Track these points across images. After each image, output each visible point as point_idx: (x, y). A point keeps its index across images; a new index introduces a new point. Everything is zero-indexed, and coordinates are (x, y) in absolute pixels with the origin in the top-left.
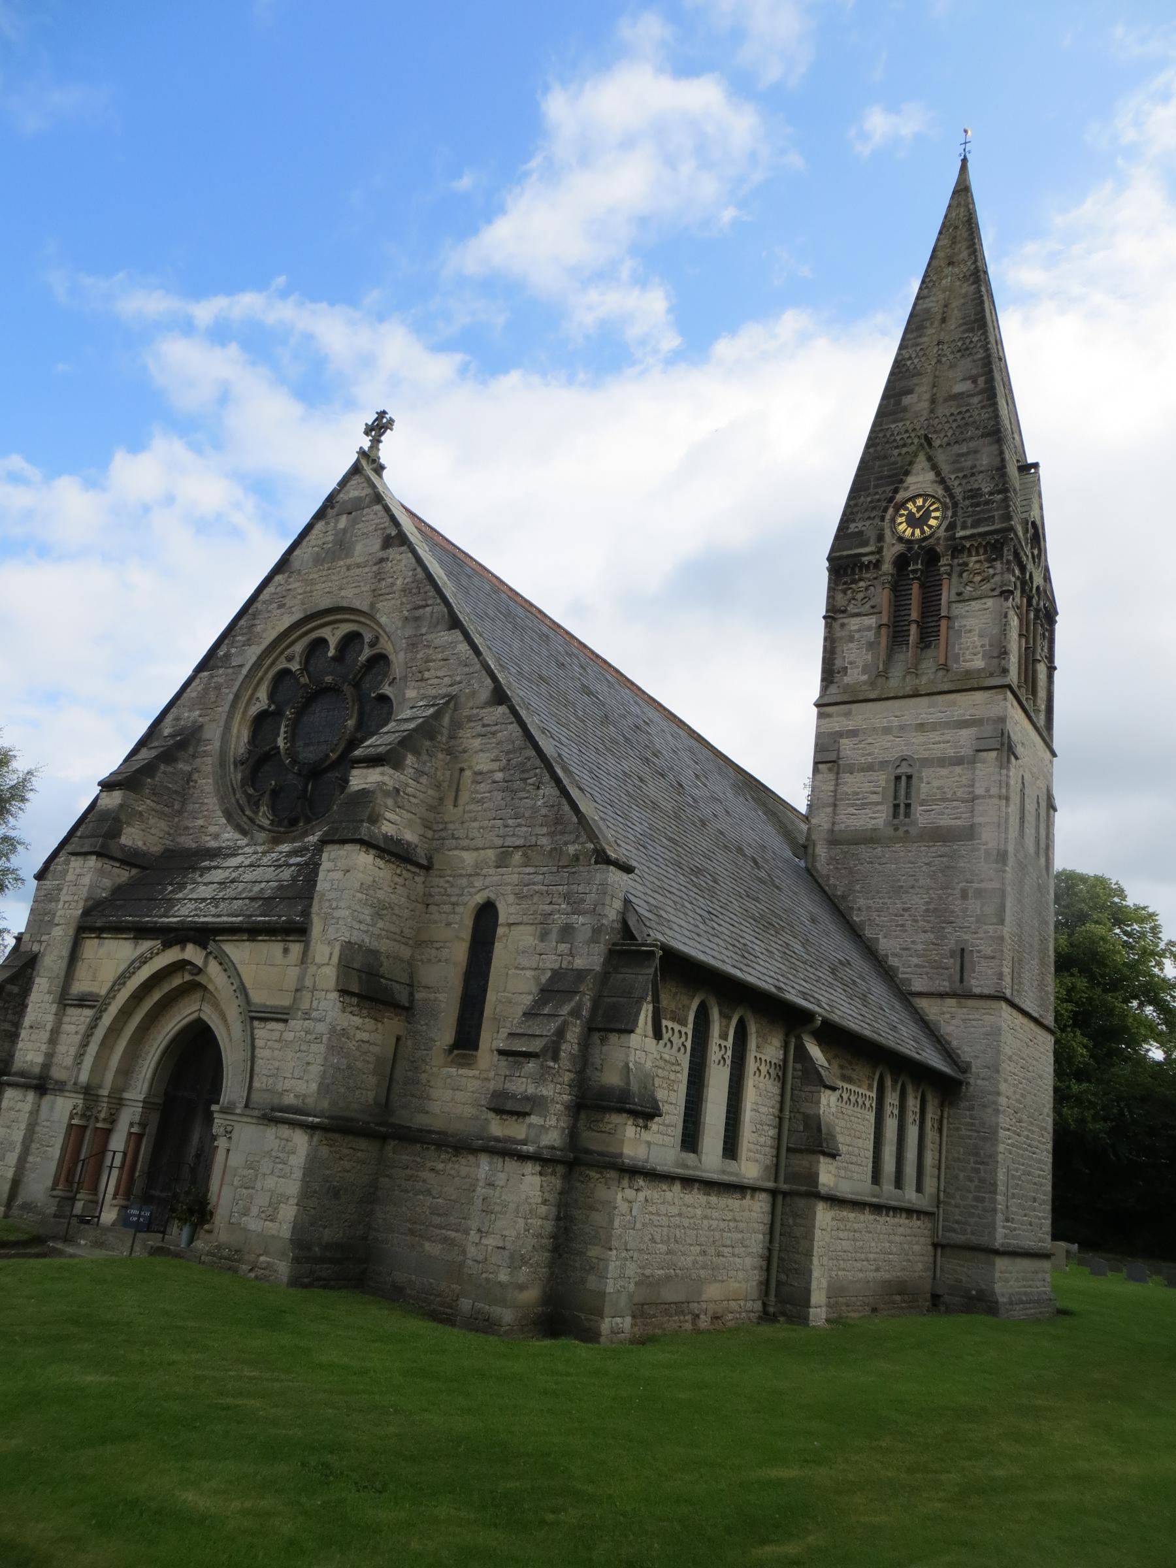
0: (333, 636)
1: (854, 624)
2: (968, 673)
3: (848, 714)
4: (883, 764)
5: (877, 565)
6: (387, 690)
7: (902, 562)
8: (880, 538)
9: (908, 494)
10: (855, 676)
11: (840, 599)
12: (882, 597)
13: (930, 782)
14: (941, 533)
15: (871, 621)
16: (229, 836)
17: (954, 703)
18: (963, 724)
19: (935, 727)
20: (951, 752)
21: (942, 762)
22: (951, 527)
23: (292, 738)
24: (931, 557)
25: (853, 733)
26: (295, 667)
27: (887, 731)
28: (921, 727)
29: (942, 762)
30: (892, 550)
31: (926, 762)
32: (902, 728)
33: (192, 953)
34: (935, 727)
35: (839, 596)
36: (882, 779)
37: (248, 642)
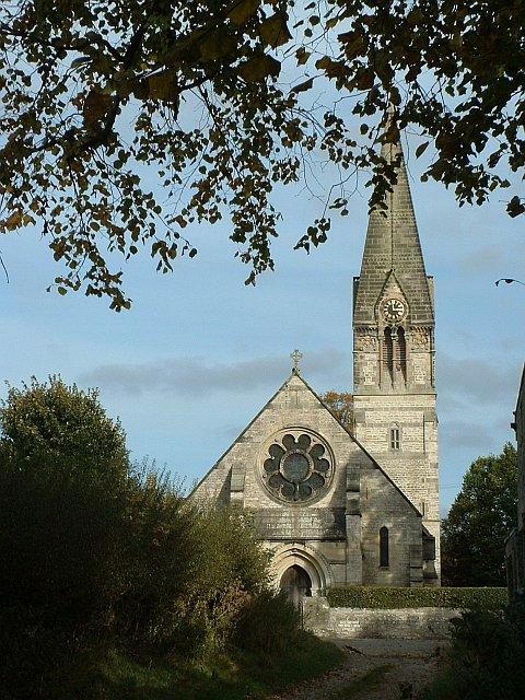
0: (297, 435)
1: (367, 357)
2: (419, 386)
3: (368, 400)
4: (386, 425)
5: (377, 330)
6: (325, 457)
7: (388, 331)
8: (376, 318)
9: (388, 298)
10: (368, 382)
11: (359, 344)
12: (380, 345)
13: (406, 432)
14: (404, 320)
15: (375, 356)
16: (273, 505)
17: (414, 399)
18: (418, 409)
19: (407, 409)
20: (414, 421)
21: (410, 425)
22: (409, 317)
23: (286, 472)
24: (401, 331)
25: (372, 410)
26: (281, 445)
27: (386, 409)
28: (401, 409)
29: (410, 425)
30: (382, 327)
31: (404, 425)
32: (393, 409)
33: (296, 546)
34: (407, 409)
35: (358, 342)
36: (386, 430)
37: (260, 434)
